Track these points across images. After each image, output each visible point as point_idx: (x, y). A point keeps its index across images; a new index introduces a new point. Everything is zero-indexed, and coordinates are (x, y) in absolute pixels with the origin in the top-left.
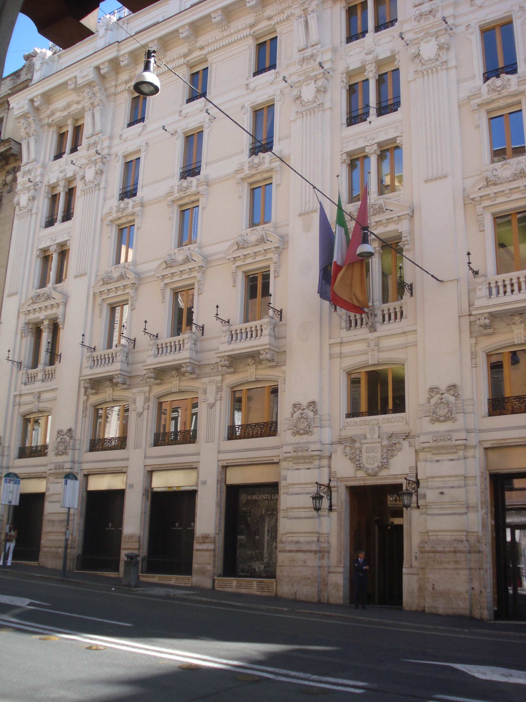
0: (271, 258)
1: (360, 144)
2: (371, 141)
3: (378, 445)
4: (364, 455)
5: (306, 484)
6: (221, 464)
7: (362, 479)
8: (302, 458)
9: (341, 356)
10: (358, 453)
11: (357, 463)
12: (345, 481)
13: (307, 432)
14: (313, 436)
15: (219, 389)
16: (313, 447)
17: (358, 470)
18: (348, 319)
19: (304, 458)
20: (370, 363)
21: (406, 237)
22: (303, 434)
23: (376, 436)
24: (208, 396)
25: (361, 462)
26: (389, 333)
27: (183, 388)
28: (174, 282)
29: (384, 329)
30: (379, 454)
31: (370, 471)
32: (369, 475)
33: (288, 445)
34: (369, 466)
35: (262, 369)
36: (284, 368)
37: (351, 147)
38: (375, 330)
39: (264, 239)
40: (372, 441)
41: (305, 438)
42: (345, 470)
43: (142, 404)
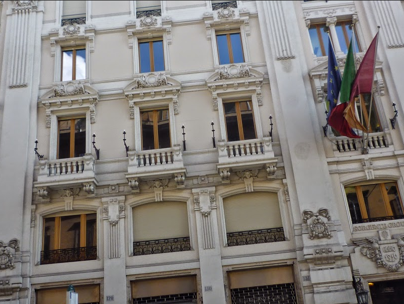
0: (255, 90)
1: (321, 15)
2: (331, 14)
3: (395, 245)
4: (384, 254)
5: (332, 282)
6: (226, 269)
7: (382, 275)
8: (325, 259)
9: (340, 173)
10: (377, 252)
11: (379, 261)
12: (367, 278)
13: (327, 236)
14: (332, 239)
15: (213, 200)
16: (335, 249)
17: (379, 267)
18: (336, 143)
19: (327, 259)
20: (368, 178)
21: (382, 84)
22: (322, 237)
23: (389, 237)
24: (201, 205)
25: (382, 260)
26: (381, 155)
27: (166, 198)
28: (144, 101)
29: (374, 152)
30: (397, 253)
31: (394, 267)
32: (392, 271)
33: (308, 247)
34: (391, 263)
35: (260, 181)
36: (284, 181)
37: (313, 16)
38: (367, 153)
39: (248, 73)
40: (386, 242)
41: (324, 242)
42: (365, 266)
43: (117, 213)
